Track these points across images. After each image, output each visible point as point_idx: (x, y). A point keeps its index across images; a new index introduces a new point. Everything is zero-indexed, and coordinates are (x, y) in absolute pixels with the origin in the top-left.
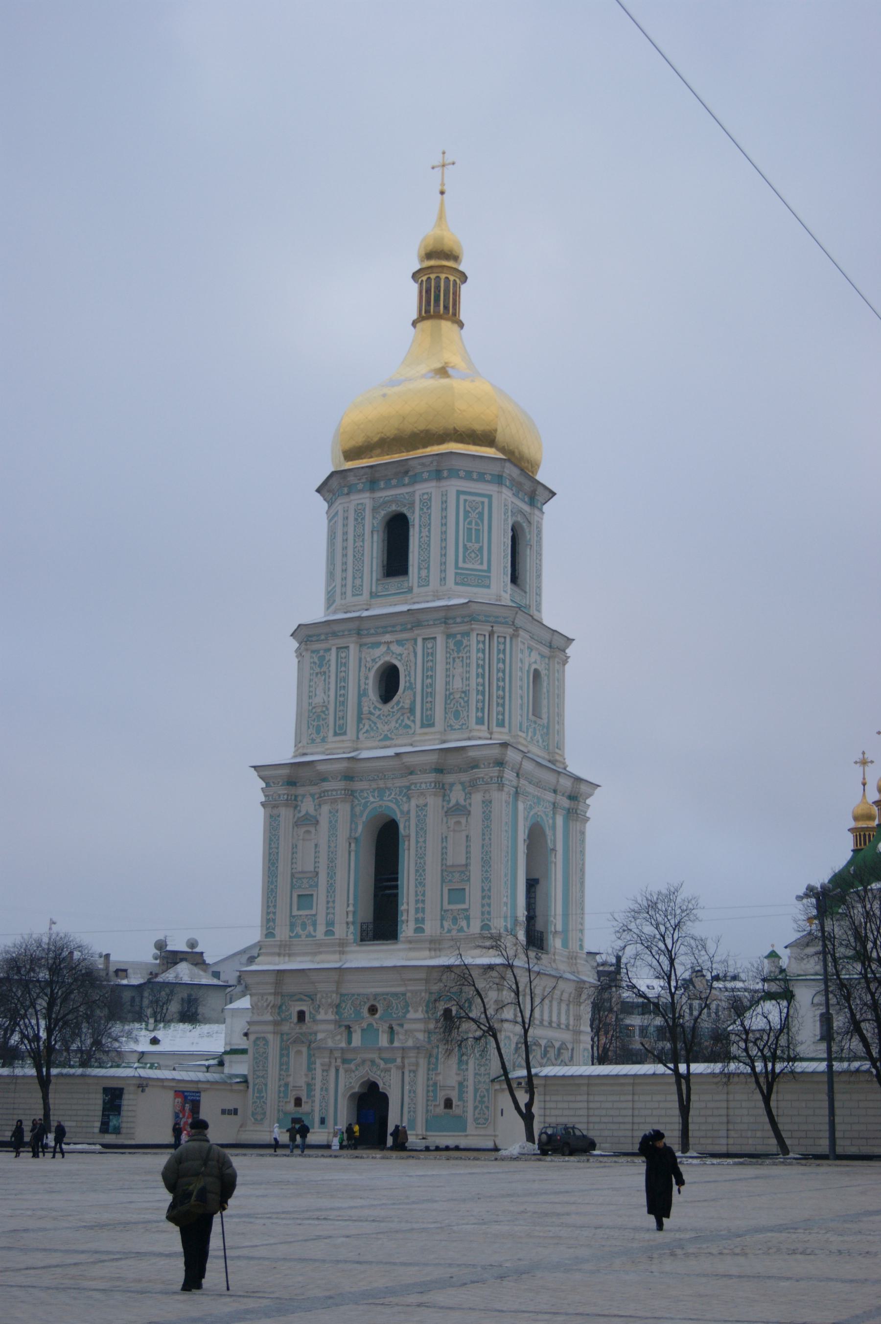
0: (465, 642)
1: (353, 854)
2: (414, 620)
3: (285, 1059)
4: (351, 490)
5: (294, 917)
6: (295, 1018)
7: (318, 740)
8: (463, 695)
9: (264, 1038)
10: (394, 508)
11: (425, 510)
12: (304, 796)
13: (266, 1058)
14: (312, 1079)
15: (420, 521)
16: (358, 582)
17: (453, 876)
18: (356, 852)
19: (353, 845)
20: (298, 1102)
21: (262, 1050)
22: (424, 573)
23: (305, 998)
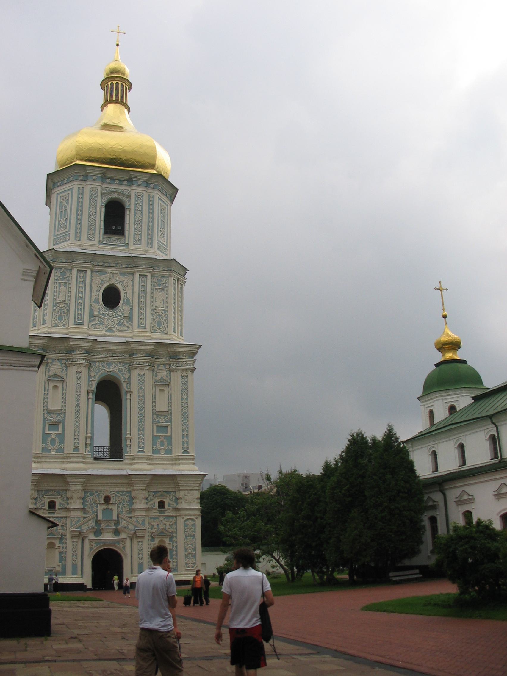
1: (90, 400)
2: (132, 263)
4: (86, 178)
7: (61, 325)
10: (116, 195)
11: (139, 201)
15: (135, 207)
16: (91, 232)
18: (92, 399)
22: (138, 237)
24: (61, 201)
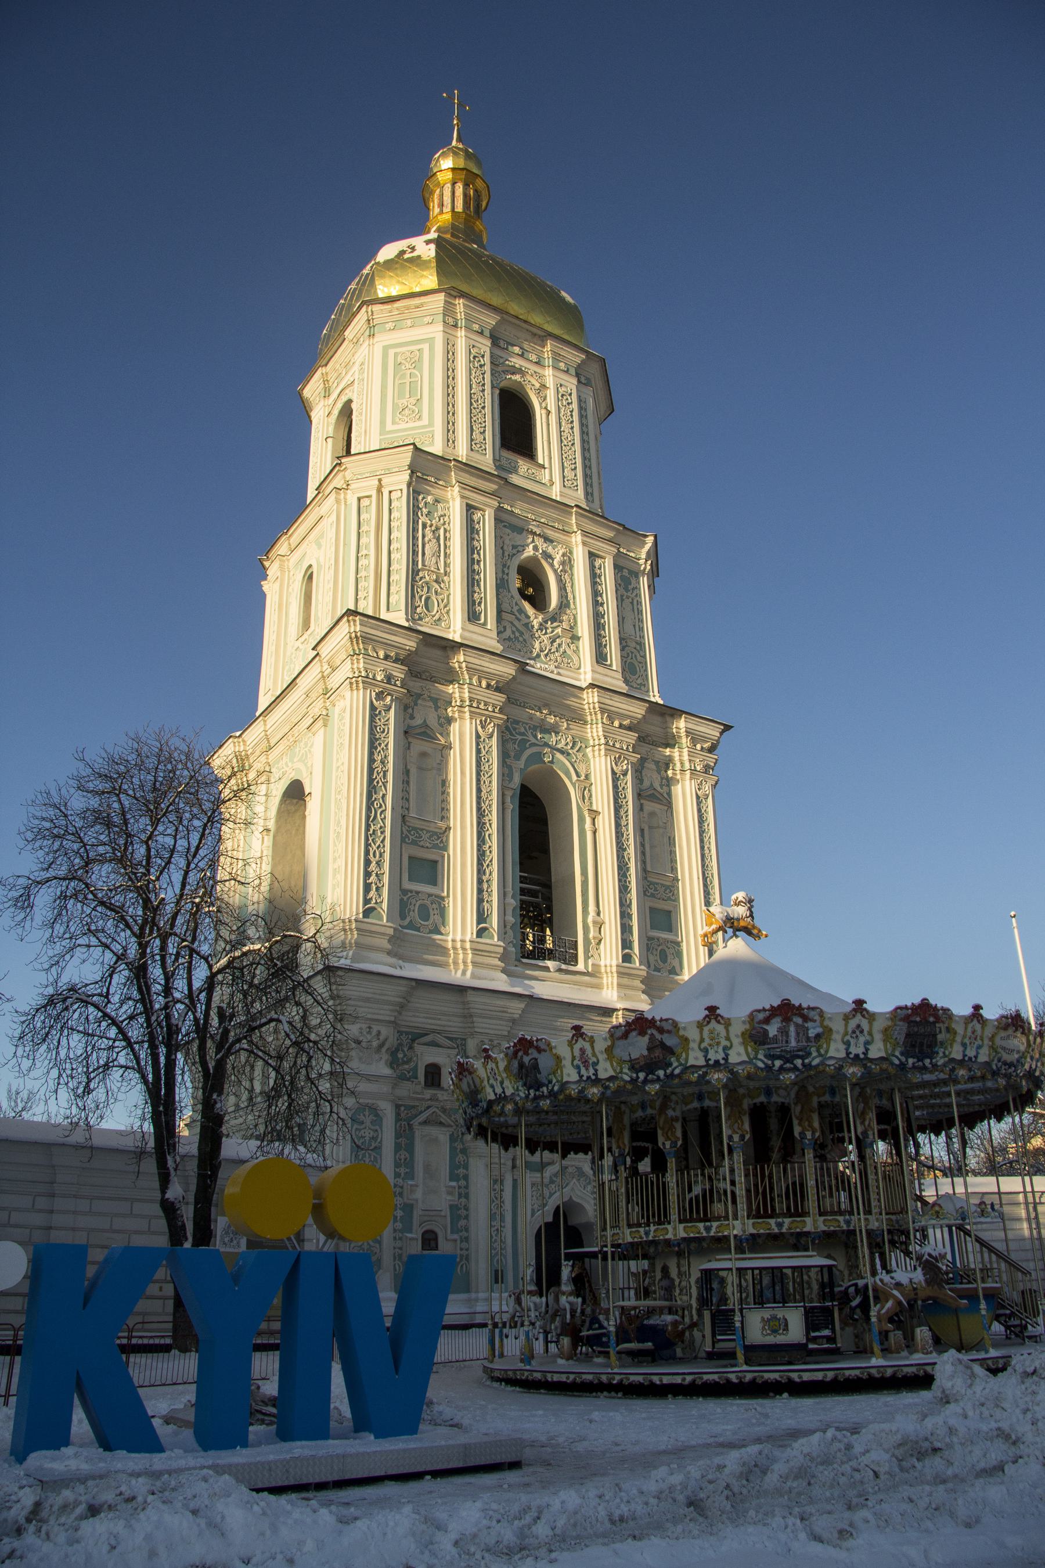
0: (633, 581)
3: (404, 1154)
5: (405, 892)
6: (421, 1077)
8: (638, 647)
9: (374, 1110)
12: (419, 696)
13: (378, 1149)
14: (460, 1196)
17: (656, 890)
19: (508, 799)
20: (430, 1240)
21: (368, 1134)
23: (448, 1043)
24: (399, 360)
